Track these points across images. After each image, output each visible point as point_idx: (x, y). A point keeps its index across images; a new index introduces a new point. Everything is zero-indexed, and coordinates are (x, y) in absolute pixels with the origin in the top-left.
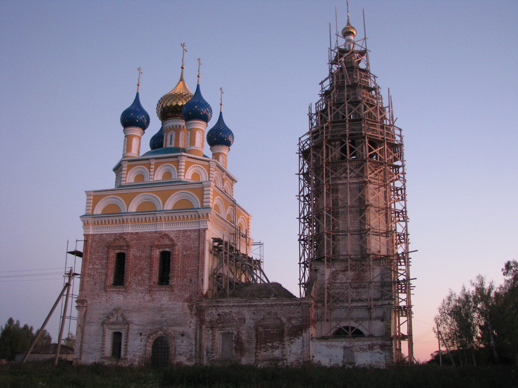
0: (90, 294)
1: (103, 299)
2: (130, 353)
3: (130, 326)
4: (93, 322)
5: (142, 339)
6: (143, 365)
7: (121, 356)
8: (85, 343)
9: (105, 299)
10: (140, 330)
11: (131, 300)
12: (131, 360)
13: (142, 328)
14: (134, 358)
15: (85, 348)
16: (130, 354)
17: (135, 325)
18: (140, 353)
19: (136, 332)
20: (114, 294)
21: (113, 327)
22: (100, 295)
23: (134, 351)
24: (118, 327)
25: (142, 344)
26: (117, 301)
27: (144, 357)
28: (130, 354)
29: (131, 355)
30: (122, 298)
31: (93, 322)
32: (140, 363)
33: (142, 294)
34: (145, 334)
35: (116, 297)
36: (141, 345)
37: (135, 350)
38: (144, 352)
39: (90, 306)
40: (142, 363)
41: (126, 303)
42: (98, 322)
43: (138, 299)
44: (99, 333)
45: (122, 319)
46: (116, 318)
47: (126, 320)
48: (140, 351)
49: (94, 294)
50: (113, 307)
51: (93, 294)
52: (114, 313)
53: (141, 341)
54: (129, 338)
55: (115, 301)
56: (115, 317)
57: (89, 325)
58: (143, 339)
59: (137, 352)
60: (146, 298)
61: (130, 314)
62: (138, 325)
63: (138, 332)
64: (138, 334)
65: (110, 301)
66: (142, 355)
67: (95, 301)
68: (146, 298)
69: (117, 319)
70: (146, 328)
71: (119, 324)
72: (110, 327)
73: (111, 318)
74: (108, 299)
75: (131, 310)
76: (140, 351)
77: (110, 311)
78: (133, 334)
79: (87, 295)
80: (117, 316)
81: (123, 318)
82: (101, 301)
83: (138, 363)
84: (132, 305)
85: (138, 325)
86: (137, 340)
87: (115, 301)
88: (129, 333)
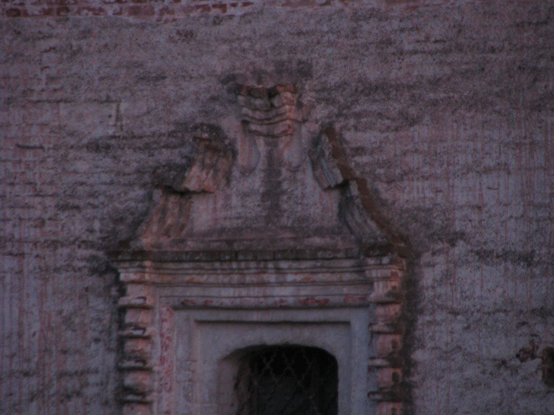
42: (55, 244)
44: (70, 365)
56: (247, 171)
63: (524, 343)
64: (533, 365)
72: (194, 293)
75: (435, 83)
78: (471, 372)
81: (343, 186)
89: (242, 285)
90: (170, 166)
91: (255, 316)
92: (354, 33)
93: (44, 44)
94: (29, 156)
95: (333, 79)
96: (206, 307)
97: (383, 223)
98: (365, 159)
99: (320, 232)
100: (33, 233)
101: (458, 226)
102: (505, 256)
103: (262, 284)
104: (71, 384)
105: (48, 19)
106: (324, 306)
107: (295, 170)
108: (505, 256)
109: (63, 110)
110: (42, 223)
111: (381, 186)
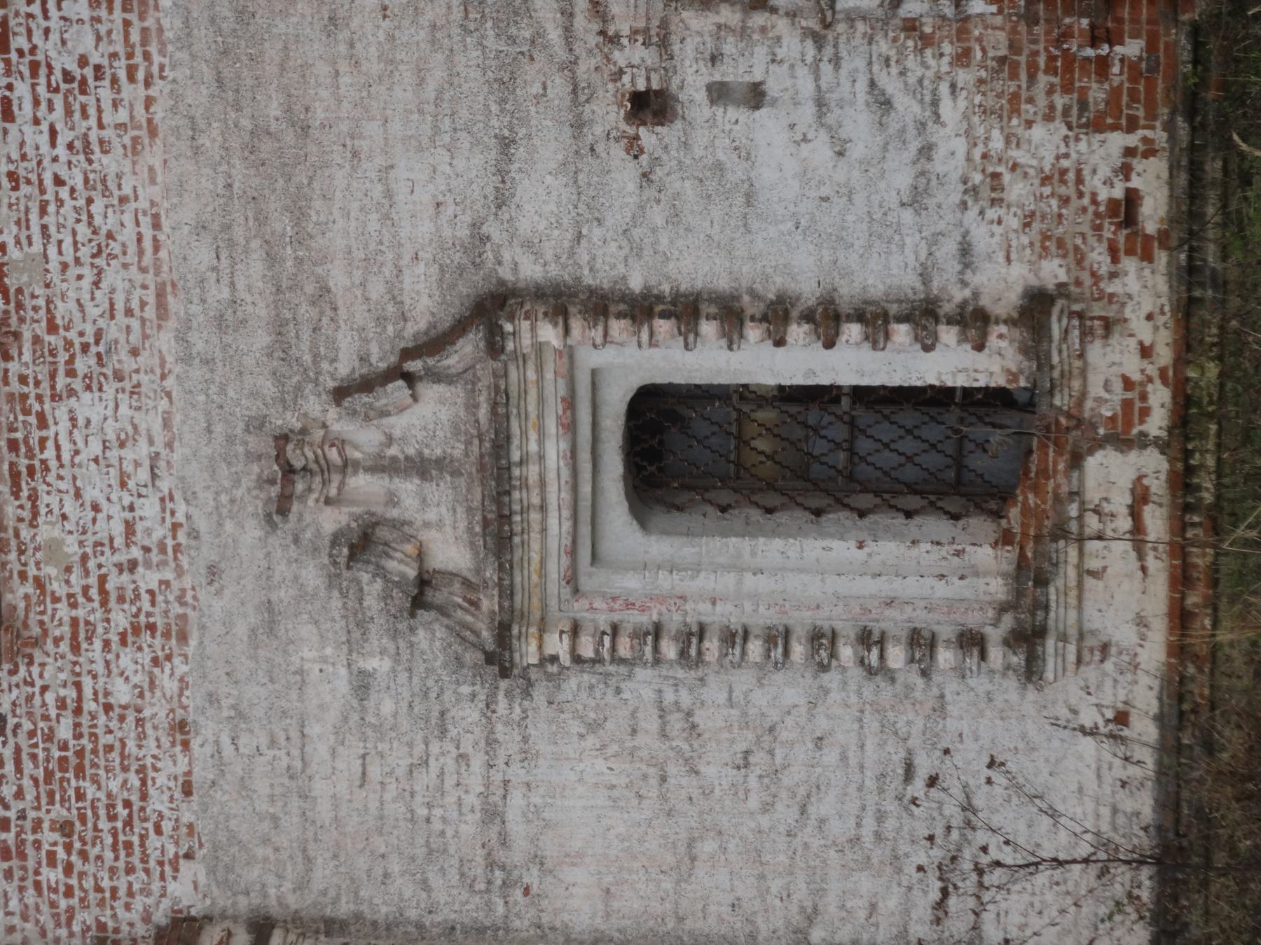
0: (52, 875)
1: (122, 693)
2: (949, 247)
3: (530, 271)
4: (492, 815)
5: (719, 93)
6: (1132, 48)
7: (1000, 381)
8: (812, 916)
9: (126, 659)
10: (579, 126)
11: (113, 277)
12: (1050, 244)
13: (559, 87)
14: (1018, 190)
15: (891, 903)
16: (965, 251)
17: (501, 201)
18: (948, 109)
19: (624, 174)
20: (46, 531)
21: (558, 525)
22: (64, 731)
23: (916, 199)
24: (555, 450)
25: (806, 86)
26: (143, 475)
27: (998, 42)
28: (965, 251)
29: (983, 237)
30: (88, 406)
31: (492, 815)
32: (1098, 94)
33: (25, 111)
34: (641, 34)
35: (89, 494)
36: (821, 104)
37: (902, 179)
38: (926, 41)
39: (253, 874)
40: (1103, 65)
41: (165, 341)
42: (491, 742)
43: (109, 163)
44: (650, 723)
45: (430, 392)
46: (408, 488)
47: (435, 343)
48: (907, 107)
49: (65, 828)
50: (253, 531)
51: (49, 836)
52: (331, 520)
53: (756, 96)
54: (723, 284)
55: (149, 508)
56: (392, 499)
57: (532, 877)
58: (729, 73)
59: (926, 151)
60: (85, 42)
61: (338, 279)
62: (506, 144)
63: (618, 151)
64: (647, 137)
65: (148, 579)
66: (964, 77)
67: (158, 803)
68: (85, 42)
69: (421, 467)
70: (554, 35)
71: (501, 444)
73: (421, 556)
74: (120, 619)
75: (272, 259)
76: (907, 107)
77: (312, 575)
78: (657, 216)
79: (84, 917)
80: (383, 466)
81: (410, 379)
82: (156, 709)
83: (1097, 126)
84: (203, 256)
85: (506, 144)
86: (746, 155)
87: (149, 508)
88: (636, 284)
89: (543, 508)
90: (386, 597)
91: (586, 489)
92: (207, 362)
93: (228, 751)
94: (375, 772)
95: (268, 388)
96: (573, 552)
97: (459, 328)
98: (374, 350)
99: (472, 407)
100: (477, 762)
101: (463, 232)
102: (502, 174)
103: (542, 483)
104: (676, 723)
105: (195, 744)
106: (570, 403)
107: (390, 440)
108: (502, 174)
109: (314, 730)
110: (462, 757)
111: (410, 329)
